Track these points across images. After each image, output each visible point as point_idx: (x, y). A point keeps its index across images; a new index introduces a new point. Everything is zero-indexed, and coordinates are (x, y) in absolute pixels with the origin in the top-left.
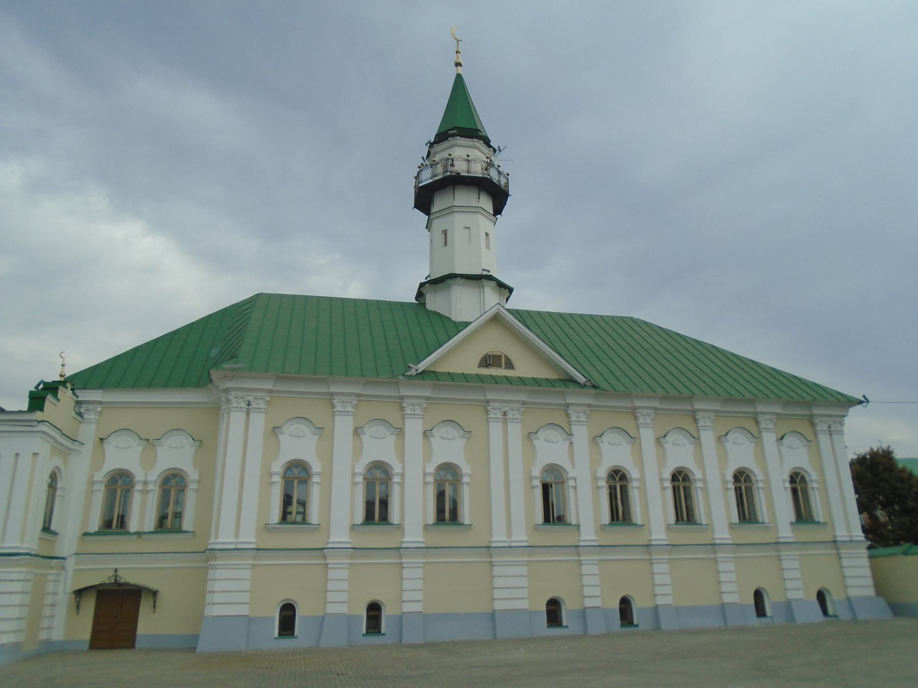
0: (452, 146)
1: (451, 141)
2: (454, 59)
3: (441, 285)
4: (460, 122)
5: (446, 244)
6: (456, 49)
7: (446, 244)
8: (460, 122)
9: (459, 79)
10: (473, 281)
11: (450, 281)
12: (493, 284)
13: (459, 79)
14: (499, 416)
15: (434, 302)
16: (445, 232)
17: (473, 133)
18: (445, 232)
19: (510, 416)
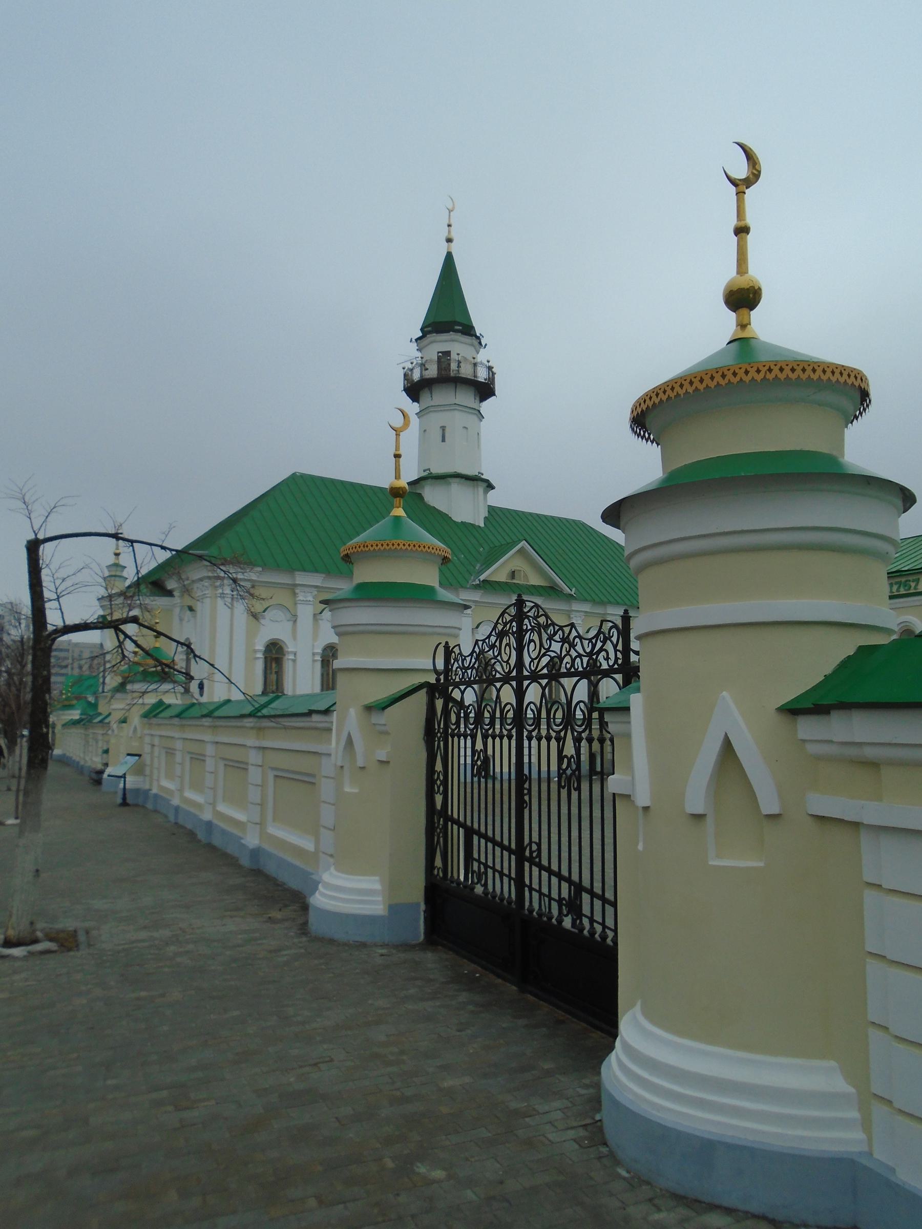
1: (452, 335)
2: (445, 235)
3: (442, 481)
5: (443, 440)
6: (447, 222)
7: (443, 440)
9: (449, 258)
10: (469, 482)
11: (450, 480)
12: (485, 485)
13: (449, 258)
15: (433, 496)
16: (443, 428)
17: (468, 330)
18: (443, 428)
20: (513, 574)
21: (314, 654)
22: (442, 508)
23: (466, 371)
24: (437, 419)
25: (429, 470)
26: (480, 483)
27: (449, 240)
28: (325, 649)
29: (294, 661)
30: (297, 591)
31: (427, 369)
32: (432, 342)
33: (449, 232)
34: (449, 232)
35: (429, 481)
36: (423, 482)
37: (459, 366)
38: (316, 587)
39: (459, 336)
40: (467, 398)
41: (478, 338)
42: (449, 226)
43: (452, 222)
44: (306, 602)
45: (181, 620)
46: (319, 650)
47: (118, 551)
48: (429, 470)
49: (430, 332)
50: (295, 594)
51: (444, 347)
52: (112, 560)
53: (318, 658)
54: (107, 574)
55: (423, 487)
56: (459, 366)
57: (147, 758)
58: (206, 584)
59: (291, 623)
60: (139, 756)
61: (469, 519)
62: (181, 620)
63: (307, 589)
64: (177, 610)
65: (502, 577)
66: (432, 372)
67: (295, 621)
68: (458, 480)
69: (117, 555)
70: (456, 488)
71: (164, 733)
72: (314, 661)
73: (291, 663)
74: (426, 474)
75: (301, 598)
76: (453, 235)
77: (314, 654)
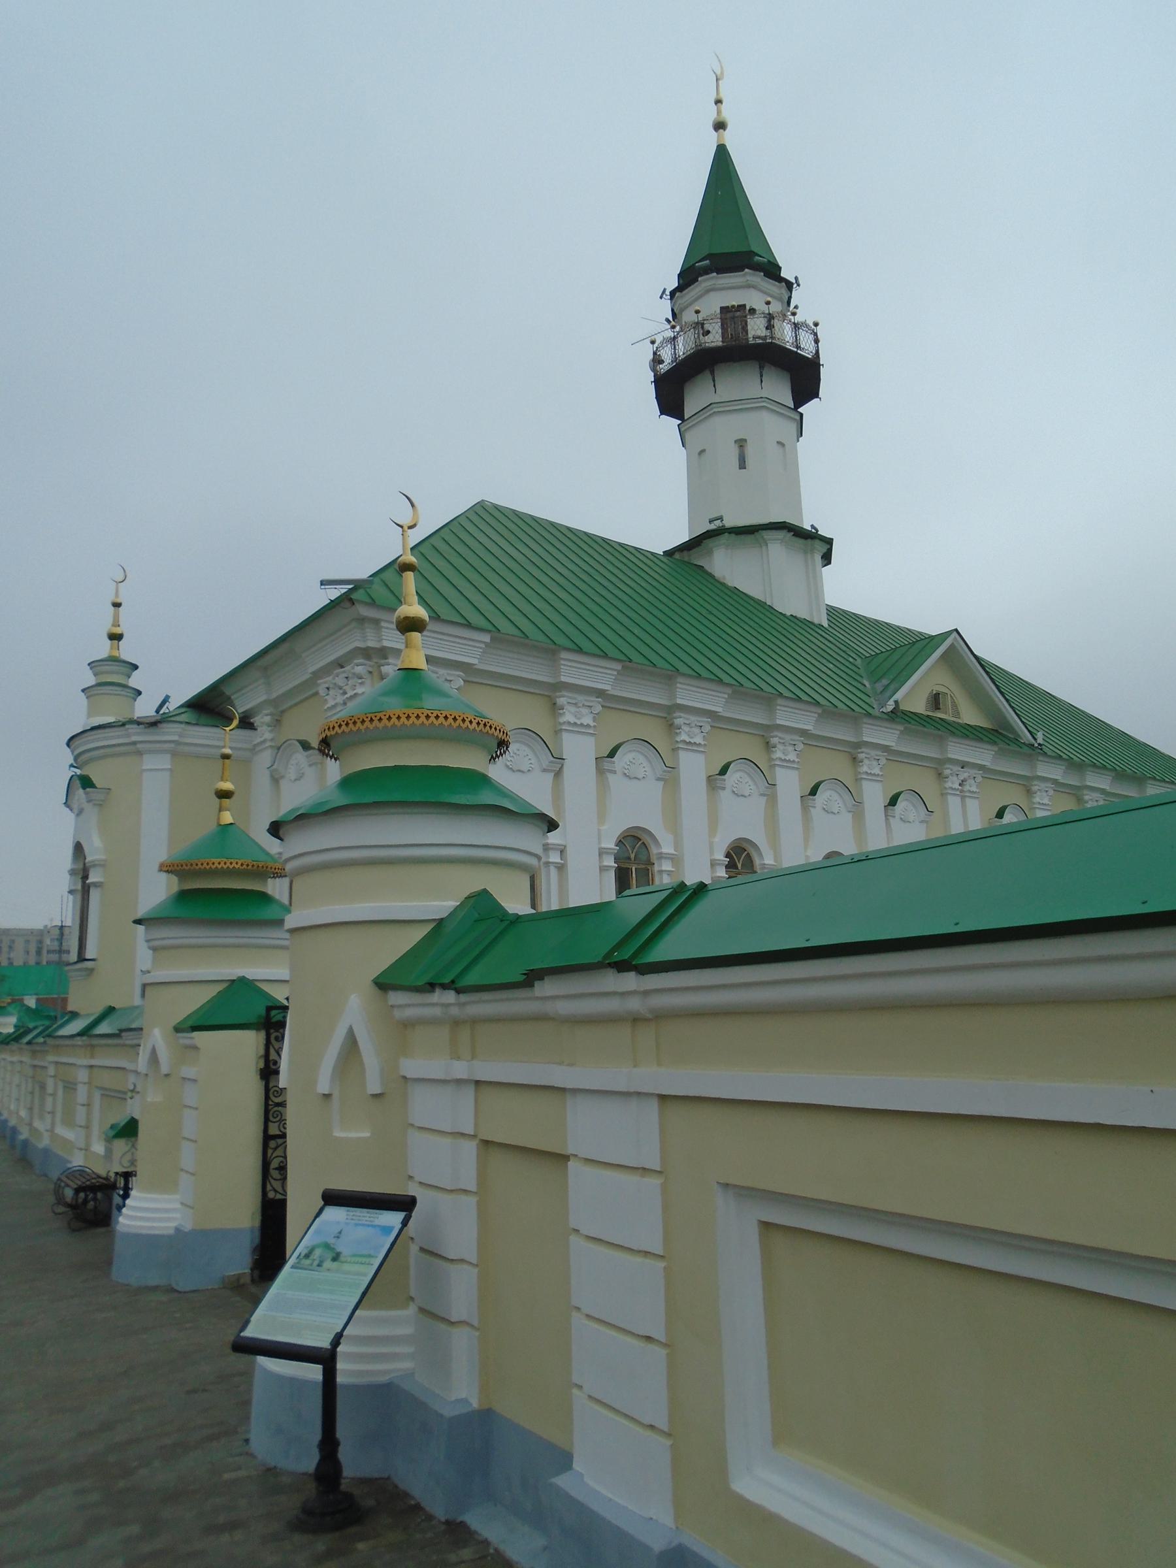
0: (749, 286)
1: (748, 276)
2: (711, 115)
3: (748, 538)
4: (726, 242)
5: (742, 465)
7: (742, 465)
8: (726, 242)
9: (722, 158)
11: (767, 535)
13: (722, 158)
14: (957, 786)
15: (730, 566)
16: (741, 443)
17: (772, 271)
18: (741, 443)
19: (967, 788)
20: (936, 700)
21: (602, 852)
22: (755, 591)
23: (785, 335)
24: (721, 431)
25: (721, 518)
26: (817, 542)
27: (720, 126)
28: (620, 843)
29: (561, 868)
30: (561, 701)
31: (708, 332)
32: (708, 291)
33: (719, 112)
34: (719, 112)
36: (709, 543)
37: (769, 327)
38: (600, 693)
39: (757, 278)
40: (779, 389)
41: (789, 286)
42: (718, 102)
43: (722, 95)
44: (579, 729)
45: (276, 780)
46: (610, 844)
47: (118, 630)
48: (721, 518)
49: (706, 271)
50: (555, 709)
51: (733, 299)
52: (104, 649)
53: (610, 862)
54: (91, 680)
55: (710, 552)
56: (769, 327)
57: (455, 1224)
58: (359, 670)
59: (551, 776)
60: (405, 1204)
61: (803, 614)
62: (276, 780)
63: (581, 698)
64: (265, 758)
65: (919, 706)
66: (715, 339)
67: (558, 774)
68: (781, 534)
69: (116, 637)
72: (603, 869)
73: (553, 871)
74: (712, 527)
75: (568, 717)
76: (727, 114)
77: (602, 852)
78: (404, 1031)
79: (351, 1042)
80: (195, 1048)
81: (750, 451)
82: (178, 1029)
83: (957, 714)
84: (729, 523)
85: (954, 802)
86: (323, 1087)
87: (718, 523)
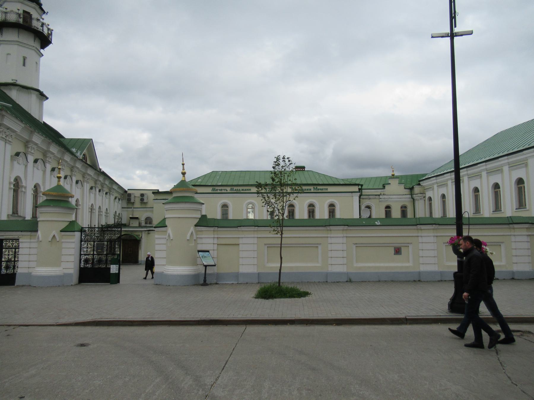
1: (34, 5)
5: (24, 65)
7: (24, 65)
16: (24, 59)
17: (40, 5)
18: (24, 59)
23: (46, 31)
35: (17, 87)
39: (37, 7)
40: (37, 45)
55: (10, 89)
66: (21, 21)
68: (37, 93)
70: (34, 97)
71: (259, 236)
74: (12, 82)
78: (197, 232)
79: (192, 233)
80: (74, 235)
81: (27, 61)
82: (61, 231)
83: (86, 161)
84: (19, 82)
85: (85, 183)
86: (188, 238)
87: (14, 81)
